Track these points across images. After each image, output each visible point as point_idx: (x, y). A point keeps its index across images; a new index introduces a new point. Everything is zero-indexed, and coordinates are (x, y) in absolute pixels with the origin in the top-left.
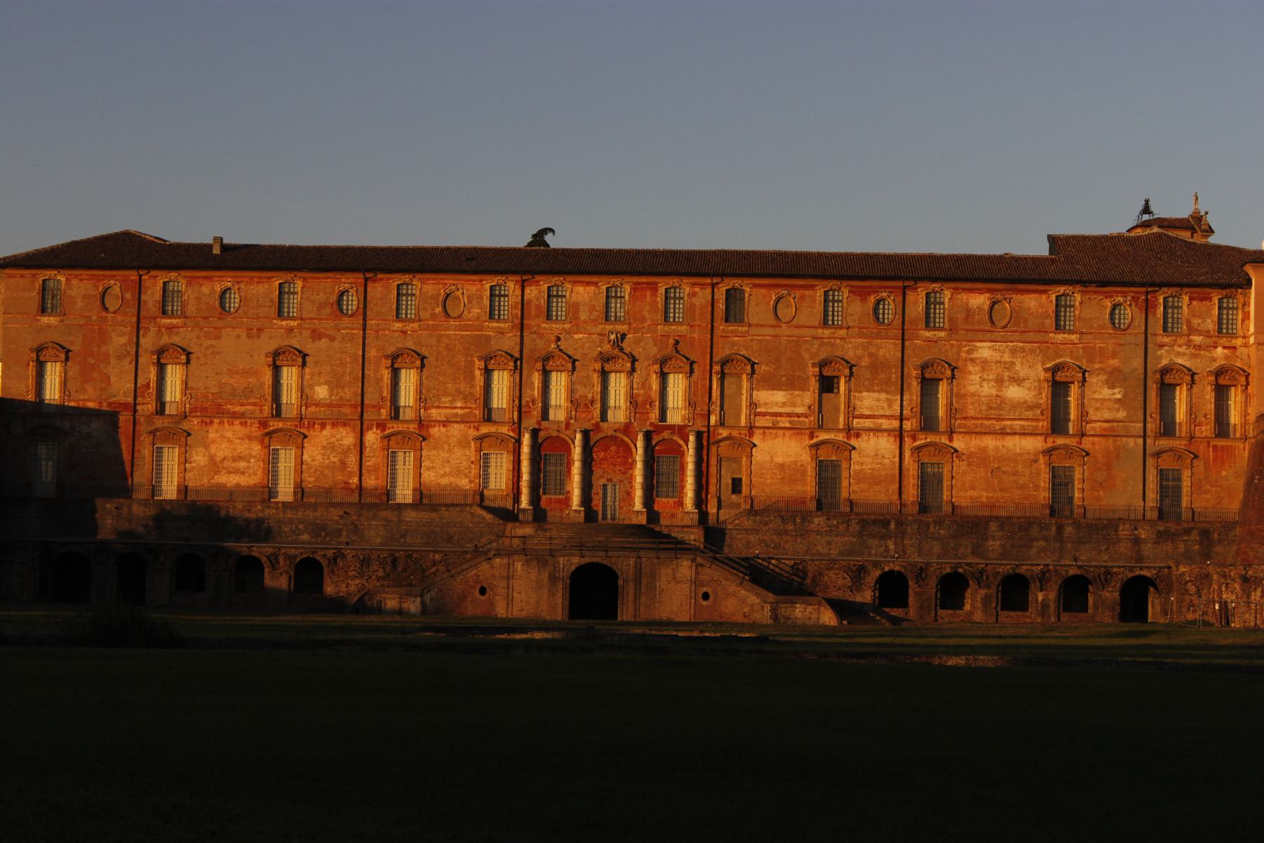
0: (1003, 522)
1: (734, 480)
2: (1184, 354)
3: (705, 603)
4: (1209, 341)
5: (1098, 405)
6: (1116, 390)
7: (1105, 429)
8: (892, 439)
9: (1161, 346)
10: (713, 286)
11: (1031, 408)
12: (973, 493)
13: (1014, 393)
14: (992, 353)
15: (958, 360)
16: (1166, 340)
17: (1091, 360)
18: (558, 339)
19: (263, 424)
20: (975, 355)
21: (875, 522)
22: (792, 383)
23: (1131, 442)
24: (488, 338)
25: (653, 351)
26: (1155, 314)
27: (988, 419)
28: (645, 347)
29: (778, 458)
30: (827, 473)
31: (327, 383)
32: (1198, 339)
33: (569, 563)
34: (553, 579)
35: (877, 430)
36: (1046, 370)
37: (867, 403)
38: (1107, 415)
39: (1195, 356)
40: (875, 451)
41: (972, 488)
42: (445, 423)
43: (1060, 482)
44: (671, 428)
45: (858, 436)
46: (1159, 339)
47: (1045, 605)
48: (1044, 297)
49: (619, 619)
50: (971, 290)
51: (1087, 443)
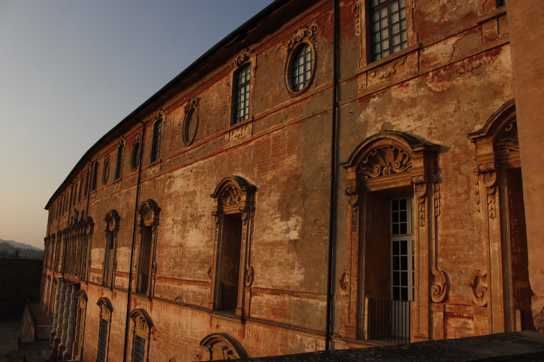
2: (413, 102)
6: (292, 222)
7: (274, 311)
9: (365, 99)
16: (374, 81)
17: (263, 170)
20: (173, 190)
26: (352, 33)
27: (173, 280)
46: (361, 81)
48: (224, 80)
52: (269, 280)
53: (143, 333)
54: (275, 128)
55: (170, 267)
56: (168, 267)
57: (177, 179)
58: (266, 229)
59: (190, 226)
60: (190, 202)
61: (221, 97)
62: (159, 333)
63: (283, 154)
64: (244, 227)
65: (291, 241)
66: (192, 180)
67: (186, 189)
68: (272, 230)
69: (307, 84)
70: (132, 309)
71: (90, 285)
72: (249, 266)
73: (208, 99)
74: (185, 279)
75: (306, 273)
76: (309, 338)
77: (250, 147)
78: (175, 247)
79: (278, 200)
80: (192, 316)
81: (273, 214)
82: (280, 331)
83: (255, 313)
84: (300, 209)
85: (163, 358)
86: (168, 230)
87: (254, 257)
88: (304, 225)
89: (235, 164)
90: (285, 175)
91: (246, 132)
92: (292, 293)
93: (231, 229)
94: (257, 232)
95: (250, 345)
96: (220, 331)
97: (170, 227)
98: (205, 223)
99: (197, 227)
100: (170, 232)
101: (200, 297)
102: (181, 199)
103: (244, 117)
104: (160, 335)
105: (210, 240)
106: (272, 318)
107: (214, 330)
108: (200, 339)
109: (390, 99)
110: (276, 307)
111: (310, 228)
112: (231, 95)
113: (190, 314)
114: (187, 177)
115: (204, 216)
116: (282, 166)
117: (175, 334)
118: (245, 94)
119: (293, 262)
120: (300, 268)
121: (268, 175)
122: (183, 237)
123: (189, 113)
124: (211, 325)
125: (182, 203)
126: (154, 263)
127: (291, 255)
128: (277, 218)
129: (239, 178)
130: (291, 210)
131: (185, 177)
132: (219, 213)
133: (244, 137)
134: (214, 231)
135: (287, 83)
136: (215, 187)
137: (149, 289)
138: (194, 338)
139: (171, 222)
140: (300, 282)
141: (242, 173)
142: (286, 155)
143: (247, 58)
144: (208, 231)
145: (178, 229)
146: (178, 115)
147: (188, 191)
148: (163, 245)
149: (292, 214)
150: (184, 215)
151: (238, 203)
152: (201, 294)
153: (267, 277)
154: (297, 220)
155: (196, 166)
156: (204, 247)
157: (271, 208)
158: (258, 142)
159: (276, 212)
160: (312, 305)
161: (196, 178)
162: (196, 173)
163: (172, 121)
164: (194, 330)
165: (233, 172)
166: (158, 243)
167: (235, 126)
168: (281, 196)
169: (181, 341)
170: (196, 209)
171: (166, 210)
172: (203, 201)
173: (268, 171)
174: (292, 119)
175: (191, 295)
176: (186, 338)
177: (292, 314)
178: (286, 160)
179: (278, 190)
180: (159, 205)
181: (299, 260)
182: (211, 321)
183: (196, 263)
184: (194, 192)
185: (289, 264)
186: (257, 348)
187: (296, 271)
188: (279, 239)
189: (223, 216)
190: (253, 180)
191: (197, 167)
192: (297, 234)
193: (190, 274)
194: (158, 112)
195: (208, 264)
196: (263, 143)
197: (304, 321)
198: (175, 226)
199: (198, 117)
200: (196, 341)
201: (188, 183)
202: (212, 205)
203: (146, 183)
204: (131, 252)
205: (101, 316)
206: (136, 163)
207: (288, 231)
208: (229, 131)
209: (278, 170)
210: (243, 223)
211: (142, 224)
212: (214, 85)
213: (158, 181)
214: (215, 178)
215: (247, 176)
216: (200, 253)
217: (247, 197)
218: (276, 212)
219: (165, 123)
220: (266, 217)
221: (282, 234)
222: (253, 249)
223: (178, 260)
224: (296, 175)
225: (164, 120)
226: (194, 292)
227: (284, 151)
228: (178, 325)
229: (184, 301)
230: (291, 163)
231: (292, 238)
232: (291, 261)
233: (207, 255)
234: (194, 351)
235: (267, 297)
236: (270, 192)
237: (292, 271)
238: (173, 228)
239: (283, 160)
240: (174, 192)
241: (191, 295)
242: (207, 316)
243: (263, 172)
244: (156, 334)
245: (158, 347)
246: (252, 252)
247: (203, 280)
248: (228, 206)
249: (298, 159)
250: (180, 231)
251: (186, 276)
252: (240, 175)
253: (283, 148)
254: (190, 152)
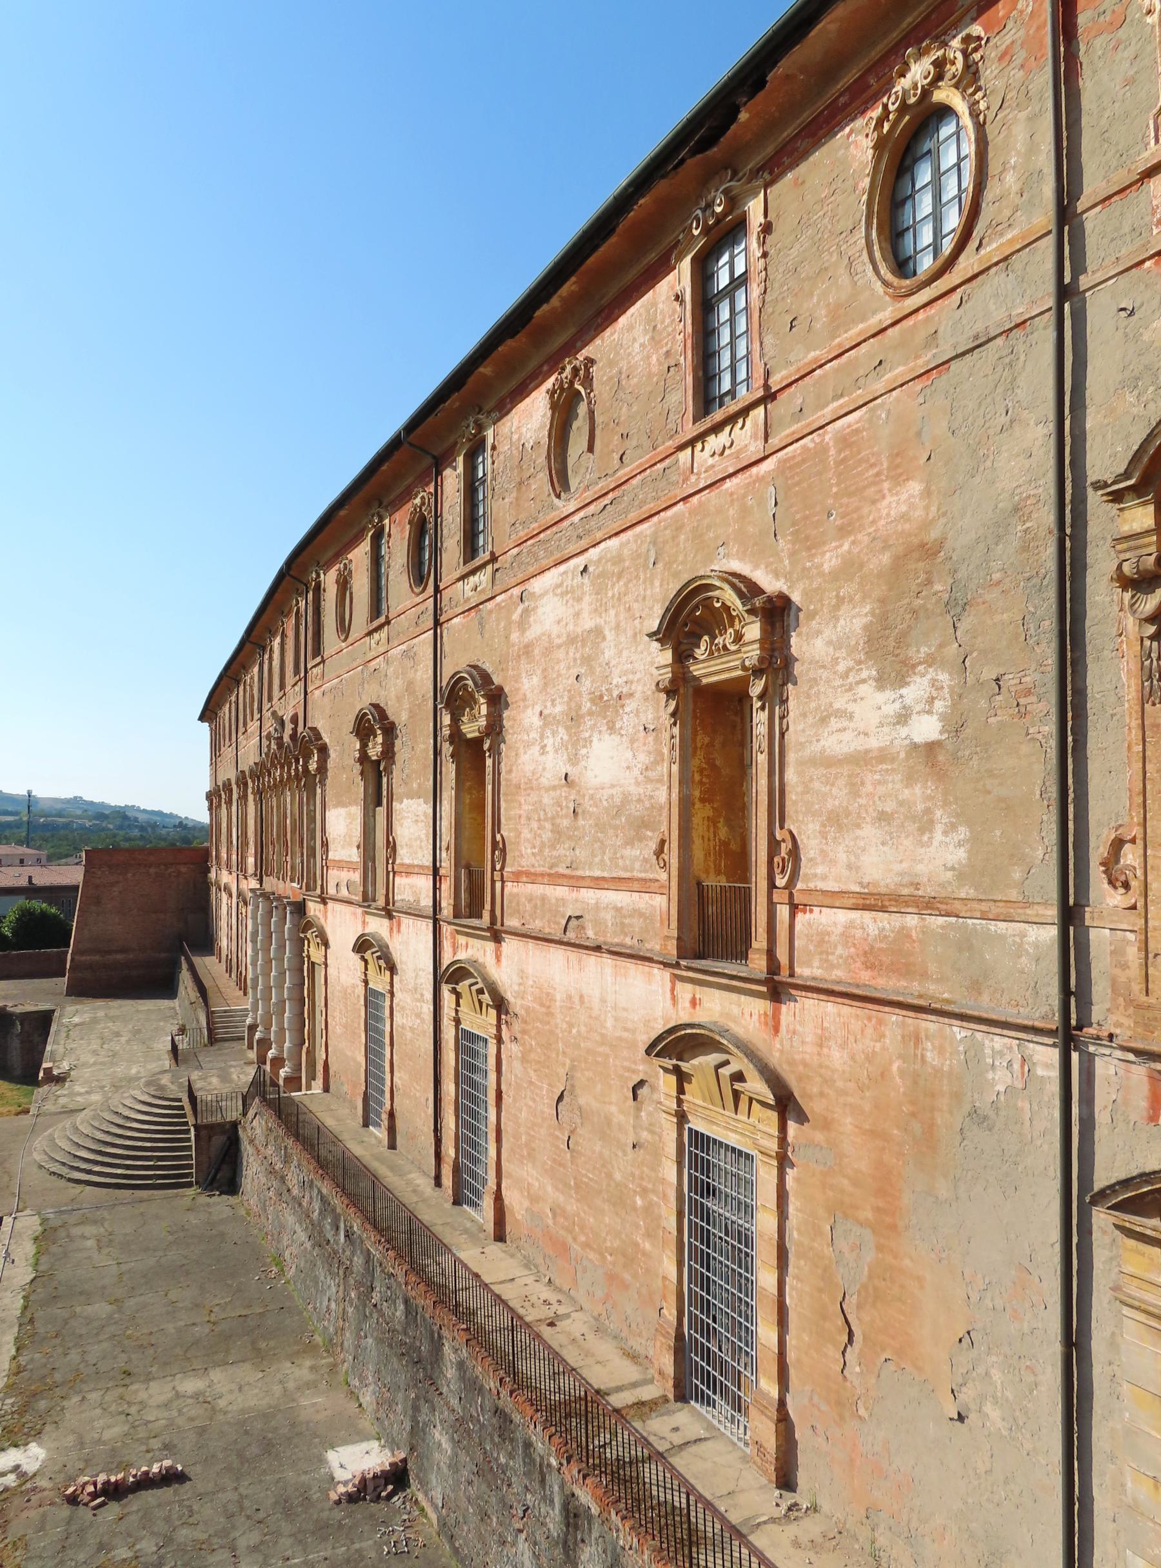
5: (838, 796)
6: (916, 690)
7: (870, 958)
27: (555, 879)
38: (877, 860)
52: (849, 867)
53: (481, 1023)
54: (841, 406)
55: (543, 845)
56: (538, 843)
57: (544, 601)
58: (829, 716)
59: (593, 728)
60: (587, 660)
61: (655, 341)
62: (525, 1022)
63: (874, 483)
64: (760, 718)
65: (915, 746)
66: (587, 599)
67: (571, 627)
68: (851, 717)
69: (947, 246)
70: (447, 959)
71: (330, 904)
72: (782, 828)
73: (617, 353)
74: (588, 873)
75: (975, 842)
76: (997, 1038)
77: (760, 479)
78: (554, 788)
79: (866, 628)
80: (616, 975)
81: (849, 670)
82: (894, 1017)
83: (809, 964)
84: (941, 646)
85: (541, 1088)
86: (528, 745)
87: (795, 803)
88: (958, 697)
89: (717, 538)
90: (886, 547)
91: (745, 437)
92: (928, 905)
93: (719, 729)
94: (800, 727)
95: (797, 1057)
96: (701, 1016)
97: (534, 735)
98: (637, 715)
99: (611, 728)
100: (536, 749)
101: (637, 923)
102: (561, 653)
103: (732, 393)
104: (529, 1027)
105: (656, 763)
106: (865, 976)
107: (684, 1017)
108: (645, 1038)
110: (878, 945)
111: (983, 703)
112: (689, 329)
113: (608, 970)
114: (573, 592)
115: (631, 695)
116: (874, 522)
117: (571, 1025)
118: (732, 321)
119: (928, 811)
120: (952, 828)
121: (828, 555)
122: (574, 760)
123: (564, 409)
124: (674, 998)
125: (562, 665)
126: (498, 837)
127: (918, 789)
128: (864, 681)
129: (734, 575)
130: (911, 652)
131: (567, 592)
132: (679, 684)
133: (739, 452)
134: (667, 736)
135: (878, 255)
136: (658, 611)
137: (488, 906)
138: (625, 1035)
139: (537, 722)
140: (953, 869)
141: (741, 560)
142: (886, 485)
143: (733, 202)
144: (645, 738)
145: (558, 739)
146: (531, 417)
147: (579, 630)
148: (518, 787)
149: (914, 666)
150: (570, 699)
151: (733, 648)
152: (637, 913)
153: (842, 857)
154: (933, 682)
155: (595, 558)
156: (638, 784)
157: (843, 653)
158: (786, 461)
159: (860, 662)
160: (1002, 937)
161: (599, 591)
162: (599, 576)
163: (515, 437)
164: (625, 1014)
165: (712, 562)
166: (503, 783)
167: (708, 422)
168: (873, 615)
169: (589, 1044)
170: (606, 678)
171: (518, 689)
172: (625, 653)
173: (824, 543)
174: (901, 369)
175: (609, 917)
176: (603, 1036)
177: (932, 968)
178: (885, 502)
179: (863, 599)
180: (497, 680)
181: (946, 803)
182: (673, 990)
183: (616, 828)
184: (598, 632)
185: (914, 818)
186: (821, 1066)
187: (938, 836)
188: (874, 743)
189: (691, 690)
190: (777, 576)
191: (599, 560)
192: (938, 726)
193: (602, 860)
194: (471, 419)
195: (653, 831)
196: (804, 461)
197: (976, 987)
198: (548, 733)
199: (591, 413)
200: (633, 1045)
201: (577, 608)
202: (652, 663)
203: (455, 620)
204: (431, 811)
205: (366, 982)
206: (422, 570)
207: (903, 718)
208: (691, 443)
209: (859, 536)
210: (757, 704)
211: (456, 736)
212: (632, 310)
213: (491, 612)
214: (657, 583)
215: (756, 567)
216: (626, 799)
217: (763, 630)
218: (860, 662)
219: (494, 448)
220: (828, 681)
221: (886, 729)
222: (791, 775)
223: (565, 823)
224: (923, 545)
225: (490, 441)
226: (618, 910)
227: (878, 474)
228: (576, 999)
229: (590, 933)
230: (904, 508)
231: (918, 739)
232: (920, 807)
233: (647, 804)
234: (628, 1070)
235: (842, 917)
236: (837, 607)
237: (925, 838)
238: (542, 737)
239: (874, 502)
240: (538, 639)
241: (608, 916)
242: (661, 976)
243: (809, 549)
244: (517, 1026)
245: (524, 1060)
246: (787, 789)
247: (643, 875)
248: (704, 661)
249: (927, 493)
250: (564, 745)
251: (591, 866)
252: (736, 566)
253: (872, 466)
254: (576, 518)
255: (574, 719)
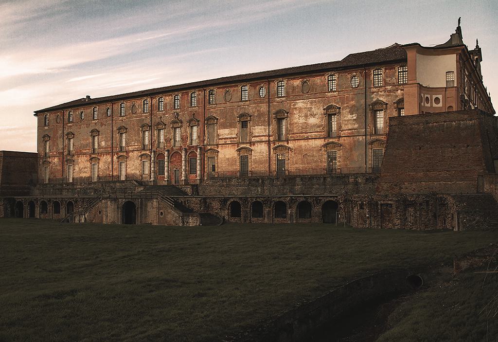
0: (303, 178)
1: (213, 165)
2: (383, 95)
3: (162, 217)
4: (394, 88)
5: (346, 123)
6: (354, 115)
7: (349, 133)
8: (266, 145)
9: (373, 93)
10: (205, 90)
11: (319, 127)
12: (297, 166)
13: (312, 121)
14: (303, 104)
15: (290, 109)
18: (161, 117)
19: (90, 156)
21: (254, 180)
22: (231, 126)
23: (361, 138)
24: (143, 119)
25: (188, 118)
28: (185, 117)
29: (227, 156)
30: (244, 161)
31: (104, 140)
32: (389, 88)
33: (122, 201)
34: (118, 208)
35: (261, 142)
36: (324, 109)
37: (257, 131)
38: (350, 127)
39: (388, 96)
40: (260, 151)
41: (296, 164)
42: (133, 151)
43: (331, 158)
44: (193, 147)
45: (254, 145)
46: (372, 89)
47: (291, 215)
48: (323, 77)
49: (138, 222)
50: (294, 79)
51: (342, 141)
109: (378, 94)
207: (353, 117)
255: (306, 116)
